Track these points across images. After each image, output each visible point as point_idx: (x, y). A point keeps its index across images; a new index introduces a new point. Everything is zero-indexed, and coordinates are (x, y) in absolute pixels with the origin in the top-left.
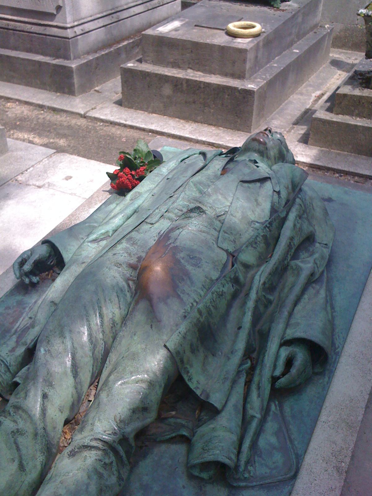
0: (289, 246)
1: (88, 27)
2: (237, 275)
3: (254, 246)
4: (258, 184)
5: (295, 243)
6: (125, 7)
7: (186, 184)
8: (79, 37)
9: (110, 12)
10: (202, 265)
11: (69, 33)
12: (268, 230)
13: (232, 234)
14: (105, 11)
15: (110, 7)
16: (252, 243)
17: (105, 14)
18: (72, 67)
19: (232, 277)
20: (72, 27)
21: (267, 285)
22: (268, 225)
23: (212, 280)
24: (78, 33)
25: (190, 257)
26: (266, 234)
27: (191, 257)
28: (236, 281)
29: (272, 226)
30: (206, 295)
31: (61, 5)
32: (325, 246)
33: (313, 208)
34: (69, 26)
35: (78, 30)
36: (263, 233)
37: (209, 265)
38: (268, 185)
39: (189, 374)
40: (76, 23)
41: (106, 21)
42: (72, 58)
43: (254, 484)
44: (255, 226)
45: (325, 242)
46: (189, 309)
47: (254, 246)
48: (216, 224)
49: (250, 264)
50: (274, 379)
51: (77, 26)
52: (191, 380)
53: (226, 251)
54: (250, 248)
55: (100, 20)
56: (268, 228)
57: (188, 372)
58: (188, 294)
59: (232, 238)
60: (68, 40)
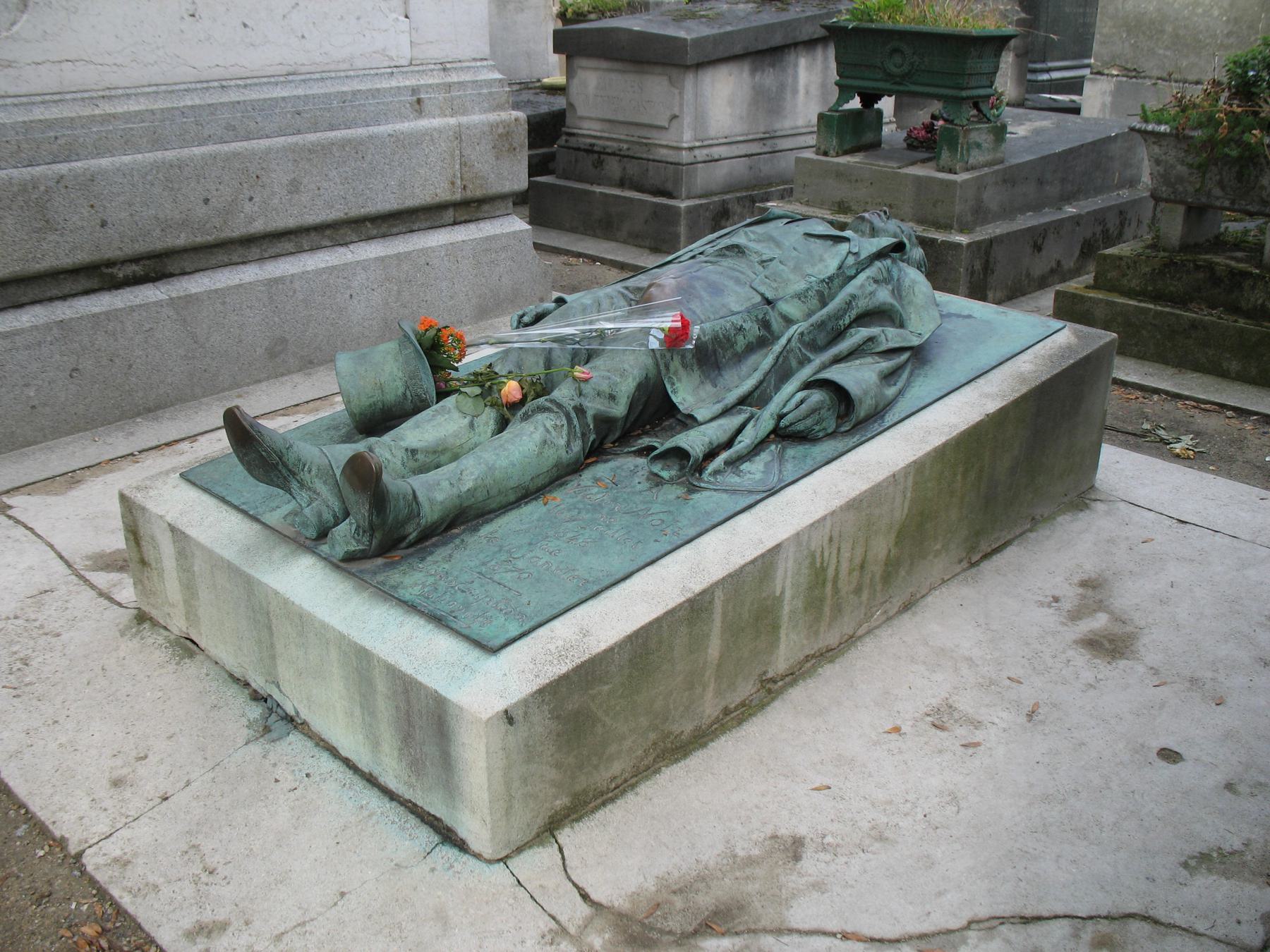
0: (849, 304)
1: (717, 152)
2: (768, 318)
3: (803, 299)
4: (830, 243)
5: (860, 306)
6: (790, 132)
8: (700, 165)
9: (762, 136)
11: (685, 157)
14: (753, 134)
15: (762, 129)
16: (801, 296)
17: (751, 137)
18: (679, 208)
19: (760, 317)
20: (691, 149)
21: (807, 339)
24: (699, 159)
28: (765, 324)
31: (677, 114)
34: (685, 145)
35: (701, 154)
38: (844, 247)
40: (697, 144)
41: (755, 148)
42: (683, 196)
43: (719, 488)
44: (810, 280)
45: (919, 332)
47: (803, 299)
49: (793, 318)
50: (781, 417)
51: (699, 147)
53: (762, 295)
54: (796, 300)
55: (741, 146)
56: (827, 283)
57: (673, 384)
59: (775, 285)
60: (680, 167)
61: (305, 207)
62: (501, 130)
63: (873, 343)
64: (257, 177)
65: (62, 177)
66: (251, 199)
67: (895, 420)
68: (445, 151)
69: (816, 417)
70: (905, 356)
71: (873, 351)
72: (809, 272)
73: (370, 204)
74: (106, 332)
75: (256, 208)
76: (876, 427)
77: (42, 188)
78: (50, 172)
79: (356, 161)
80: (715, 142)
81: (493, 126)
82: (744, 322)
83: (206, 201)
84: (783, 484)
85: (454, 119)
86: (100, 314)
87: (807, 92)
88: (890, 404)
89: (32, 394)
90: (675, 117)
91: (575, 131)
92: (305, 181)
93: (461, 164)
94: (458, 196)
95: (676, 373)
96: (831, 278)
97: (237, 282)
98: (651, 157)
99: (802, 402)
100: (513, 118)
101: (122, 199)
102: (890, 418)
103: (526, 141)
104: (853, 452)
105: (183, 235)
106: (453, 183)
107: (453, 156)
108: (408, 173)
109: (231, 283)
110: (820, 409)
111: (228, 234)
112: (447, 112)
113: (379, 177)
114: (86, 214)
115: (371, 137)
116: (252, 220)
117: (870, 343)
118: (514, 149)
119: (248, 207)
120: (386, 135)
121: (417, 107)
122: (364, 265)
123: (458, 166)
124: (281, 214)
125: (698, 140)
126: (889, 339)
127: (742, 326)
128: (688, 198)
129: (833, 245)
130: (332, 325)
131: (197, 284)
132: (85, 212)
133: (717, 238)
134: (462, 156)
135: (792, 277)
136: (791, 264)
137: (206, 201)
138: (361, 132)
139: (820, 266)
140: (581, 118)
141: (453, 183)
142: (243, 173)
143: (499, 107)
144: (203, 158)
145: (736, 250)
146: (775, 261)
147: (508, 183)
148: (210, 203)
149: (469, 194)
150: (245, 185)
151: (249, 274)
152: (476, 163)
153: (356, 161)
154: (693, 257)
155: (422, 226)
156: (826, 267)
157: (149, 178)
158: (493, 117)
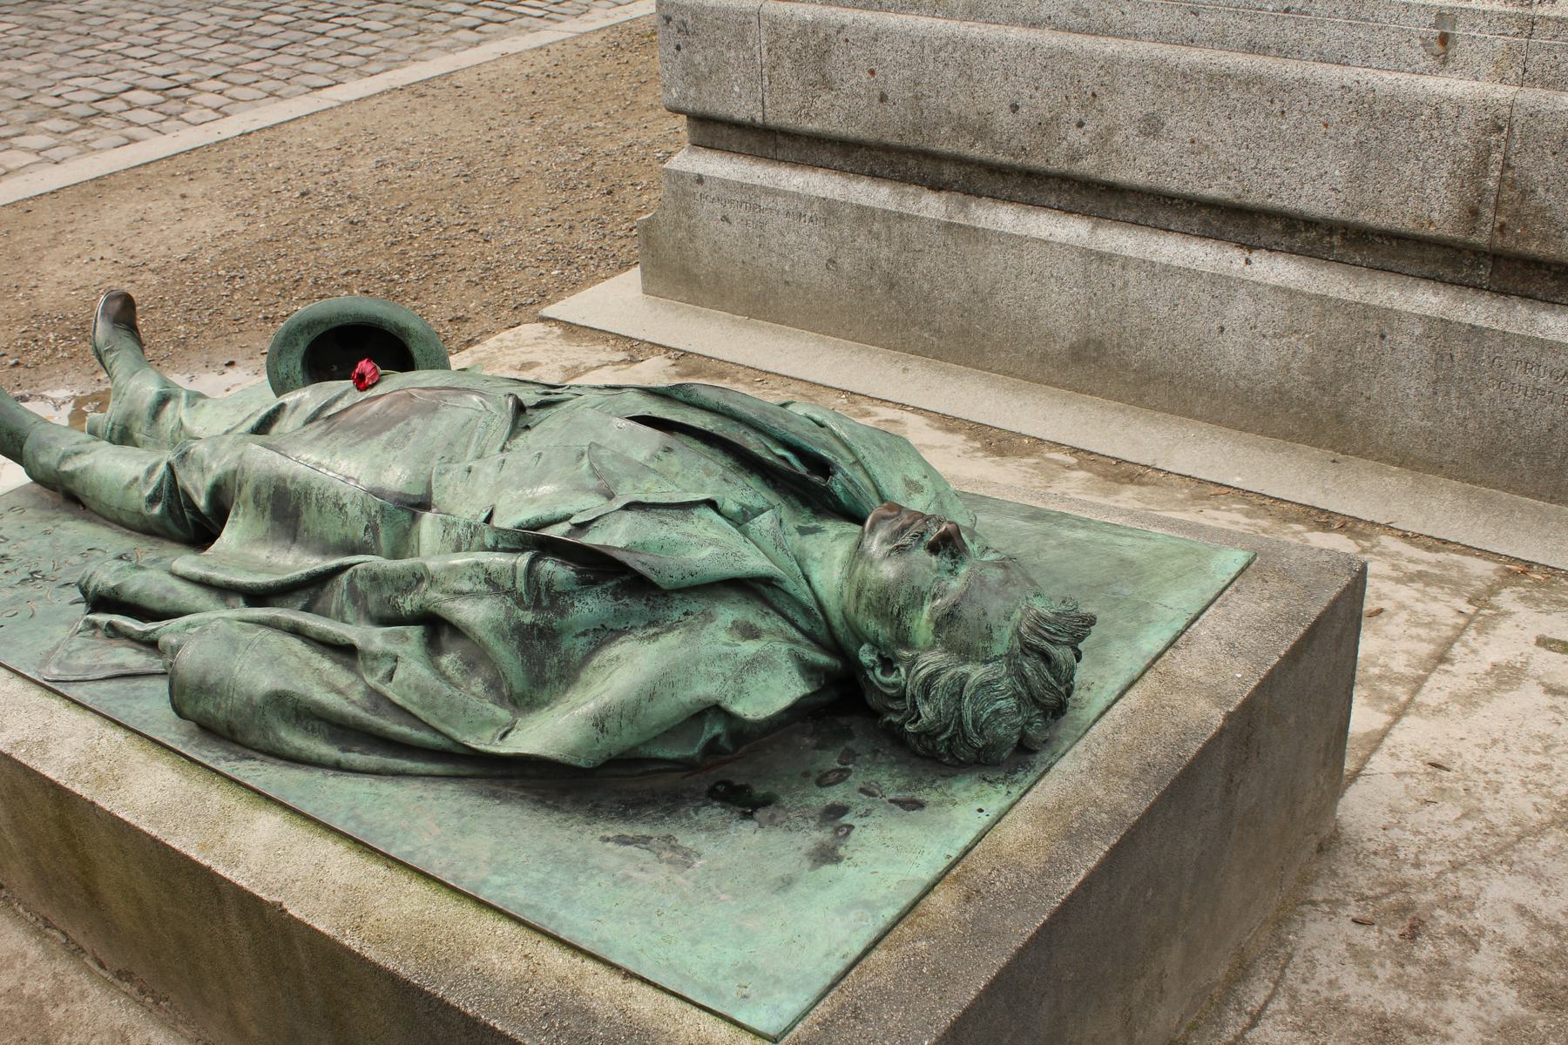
61: (1166, 163)
64: (1094, 95)
65: (843, 27)
66: (1080, 125)
68: (1466, 147)
73: (1284, 195)
74: (870, 232)
75: (1085, 140)
77: (822, 35)
78: (833, 18)
79: (1267, 115)
82: (352, 503)
83: (1015, 108)
86: (867, 208)
89: (787, 268)
92: (1170, 123)
93: (1502, 180)
94: (1481, 239)
95: (245, 502)
97: (1044, 235)
101: (907, 73)
105: (979, 145)
106: (1475, 213)
107: (1482, 161)
108: (1373, 164)
109: (1034, 233)
111: (1037, 162)
112: (1511, 74)
113: (1310, 153)
114: (864, 80)
115: (1304, 83)
116: (1074, 157)
119: (1074, 135)
120: (1337, 85)
121: (1438, 48)
122: (1256, 290)
124: (1124, 161)
127: (344, 505)
130: (1181, 358)
131: (1003, 218)
132: (865, 76)
134: (1507, 166)
137: (1015, 108)
138: (1292, 69)
141: (1475, 213)
142: (1071, 83)
144: (1016, 47)
148: (1020, 111)
149: (1508, 243)
150: (1073, 102)
151: (1072, 230)
152: (1541, 190)
153: (1267, 115)
155: (1413, 270)
157: (942, 54)
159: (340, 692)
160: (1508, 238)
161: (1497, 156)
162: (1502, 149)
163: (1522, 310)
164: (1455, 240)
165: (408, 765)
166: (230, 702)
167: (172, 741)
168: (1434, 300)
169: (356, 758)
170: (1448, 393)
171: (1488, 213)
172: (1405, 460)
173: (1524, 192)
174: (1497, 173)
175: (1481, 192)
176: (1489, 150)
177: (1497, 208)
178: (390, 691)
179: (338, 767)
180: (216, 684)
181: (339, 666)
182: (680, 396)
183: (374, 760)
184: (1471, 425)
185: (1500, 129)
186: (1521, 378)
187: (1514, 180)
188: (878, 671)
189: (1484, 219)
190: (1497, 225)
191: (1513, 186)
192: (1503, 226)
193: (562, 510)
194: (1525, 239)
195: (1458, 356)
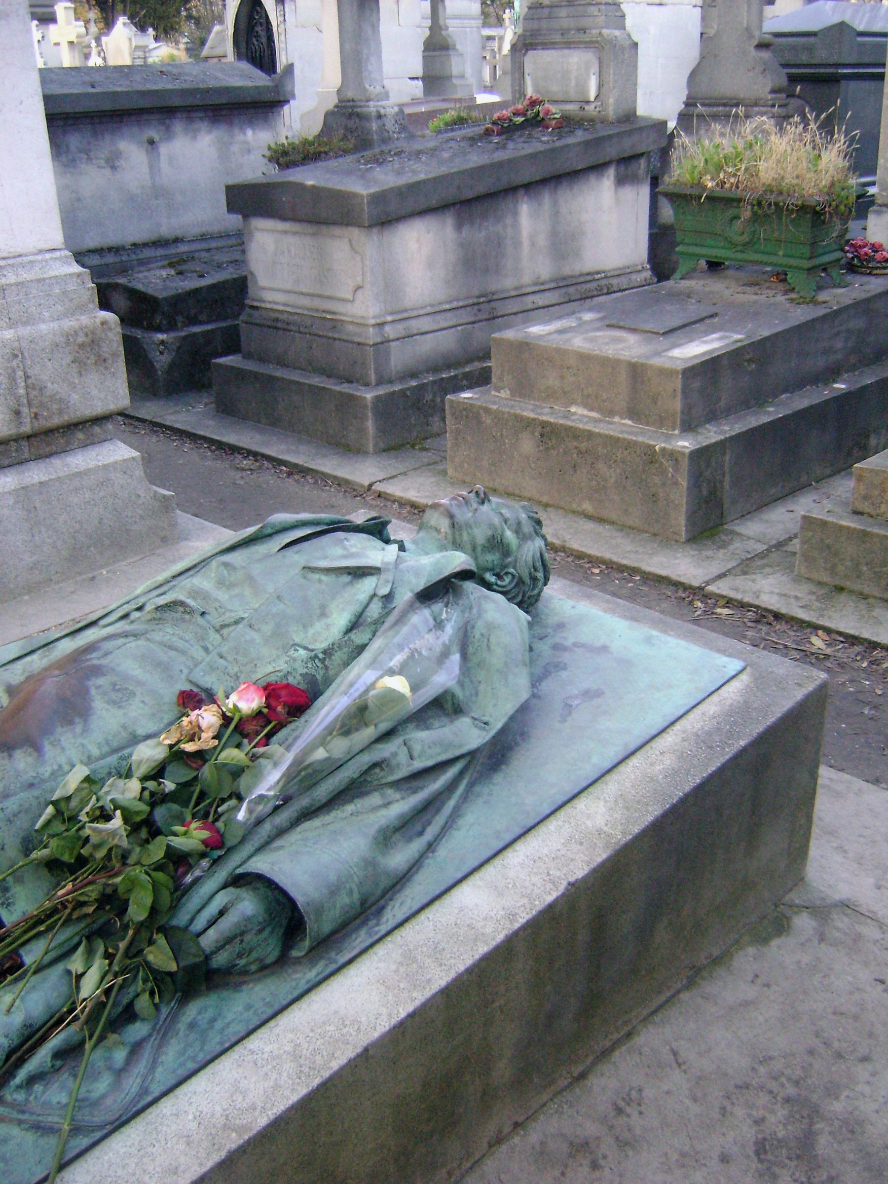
4: (346, 579)
6: (513, 293)
7: (203, 564)
8: (393, 344)
9: (475, 300)
10: (130, 704)
12: (319, 664)
13: (237, 662)
15: (477, 293)
18: (365, 398)
22: (321, 656)
23: (135, 737)
25: (114, 688)
26: (313, 672)
27: (117, 687)
29: (330, 658)
30: (102, 757)
32: (483, 725)
33: (488, 646)
36: (305, 670)
37: (146, 707)
39: (8, 895)
40: (389, 318)
44: (296, 655)
45: (486, 719)
46: (47, 775)
48: (211, 639)
51: (392, 322)
52: (8, 905)
56: (322, 661)
58: (63, 749)
59: (233, 669)
62: (81, 339)
63: (382, 769)
67: (400, 917)
69: (236, 947)
70: (452, 772)
71: (384, 781)
72: (297, 640)
76: (361, 939)
80: (415, 313)
81: (69, 337)
84: (149, 1098)
85: (12, 331)
87: (533, 244)
88: (401, 880)
90: (359, 287)
91: (256, 304)
93: (27, 387)
94: (27, 429)
96: (328, 652)
98: (336, 336)
99: (222, 913)
100: (98, 321)
102: (394, 912)
103: (122, 349)
104: (303, 1004)
106: (17, 413)
107: (12, 378)
110: (242, 934)
117: (377, 770)
118: (105, 360)
123: (22, 391)
125: (391, 314)
126: (415, 754)
128: (379, 383)
129: (350, 583)
133: (174, 577)
134: (27, 377)
135: (265, 651)
136: (267, 629)
139: (318, 626)
140: (264, 288)
141: (17, 413)
143: (81, 308)
145: (182, 609)
146: (241, 626)
147: (100, 403)
152: (49, 385)
154: (125, 616)
156: (328, 626)
158: (69, 324)
159: (389, 803)
160: (41, 421)
161: (20, 373)
162: (22, 368)
163: (56, 462)
164: (11, 435)
165: (451, 803)
166: (356, 879)
167: (318, 974)
168: (8, 479)
169: (429, 835)
170: (40, 532)
171: (25, 410)
172: (33, 589)
173: (41, 389)
174: (23, 384)
175: (18, 398)
176: (14, 371)
177: (30, 405)
178: (419, 764)
179: (431, 847)
180: (339, 877)
181: (355, 801)
182: (269, 531)
183: (439, 821)
184: (59, 543)
185: (16, 356)
186: (76, 500)
187: (33, 384)
188: (499, 583)
189: (24, 415)
190: (33, 415)
191: (34, 388)
192: (36, 415)
193: (363, 597)
194: (50, 417)
195: (38, 505)
